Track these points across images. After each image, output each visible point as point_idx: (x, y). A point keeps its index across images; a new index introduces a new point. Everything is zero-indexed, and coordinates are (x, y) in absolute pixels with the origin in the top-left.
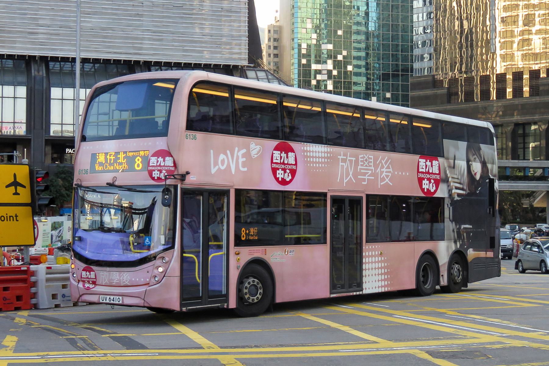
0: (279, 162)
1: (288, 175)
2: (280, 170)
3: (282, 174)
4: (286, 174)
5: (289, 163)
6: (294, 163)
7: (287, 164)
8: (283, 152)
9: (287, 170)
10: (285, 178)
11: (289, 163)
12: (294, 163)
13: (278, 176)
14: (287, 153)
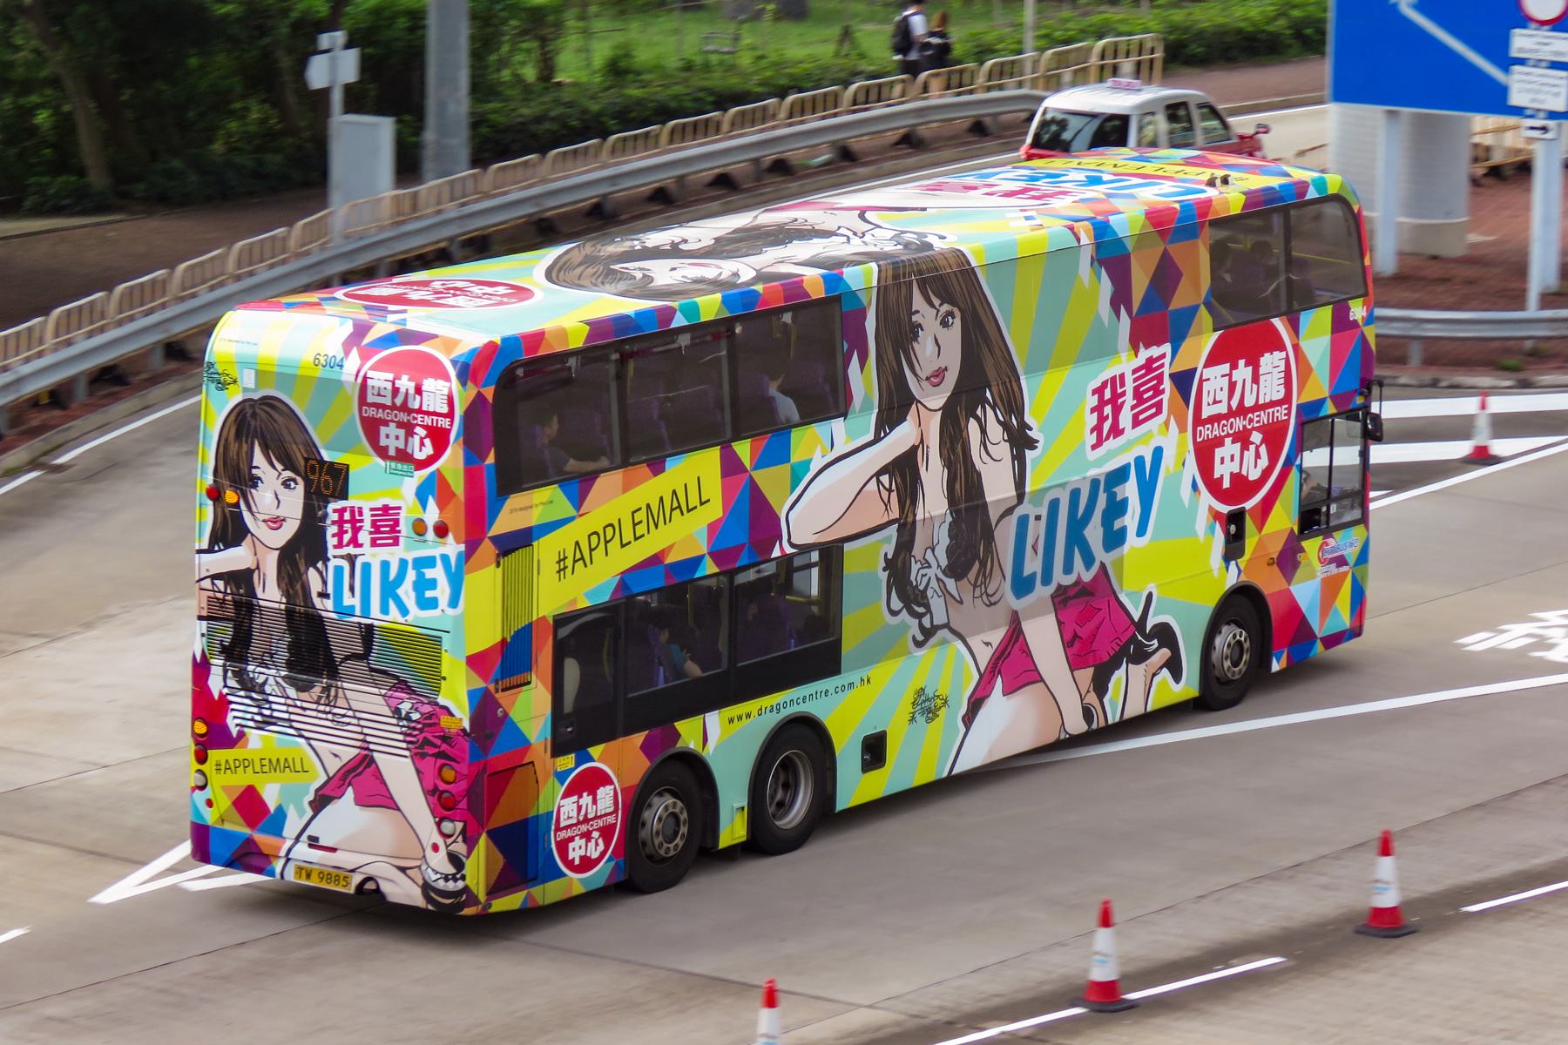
0: (389, 403)
1: (422, 444)
3: (397, 437)
6: (445, 410)
7: (420, 411)
11: (424, 408)
12: (445, 410)
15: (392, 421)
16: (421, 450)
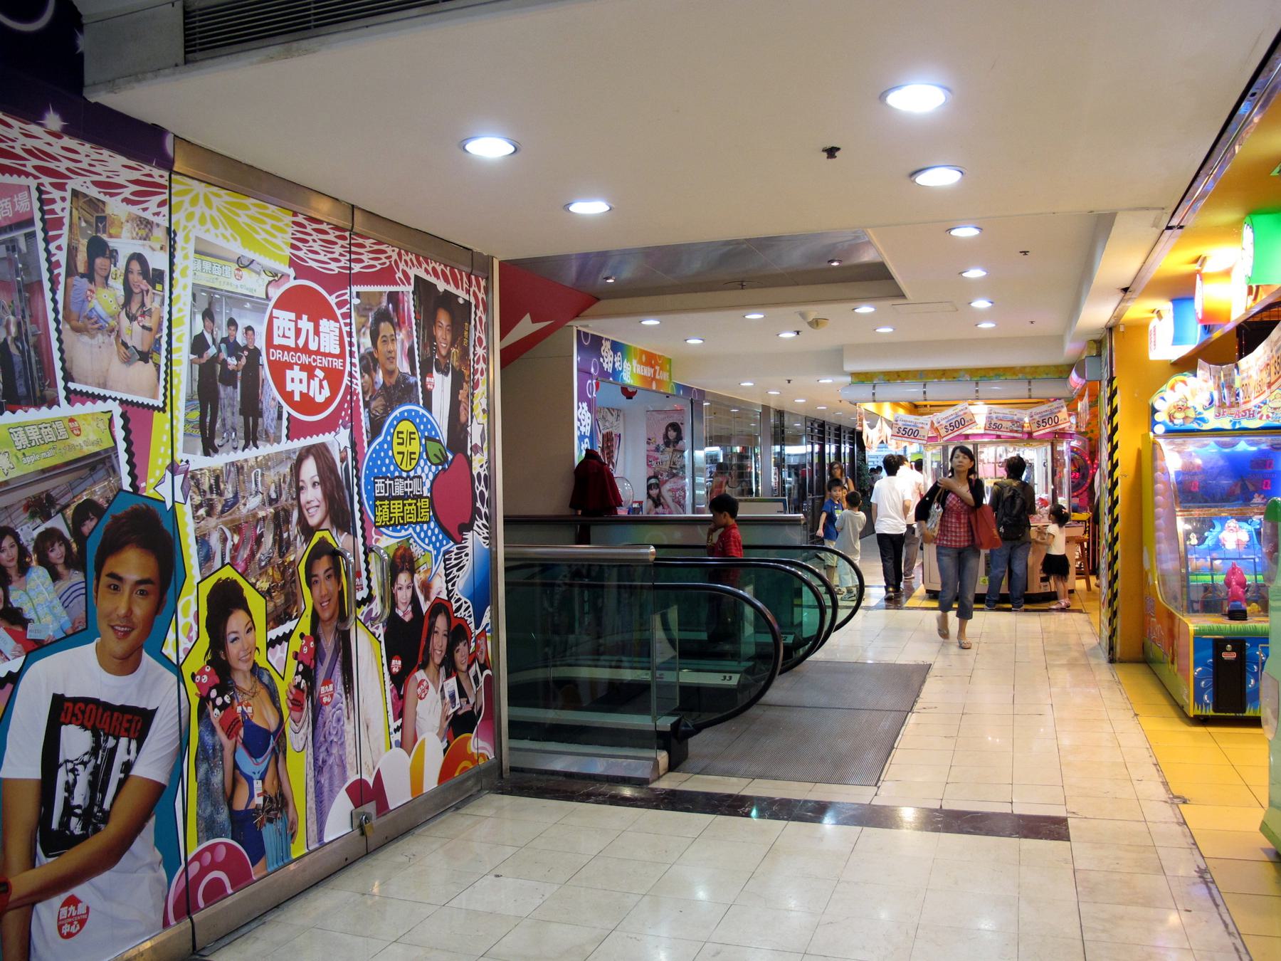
0: (293, 345)
1: (321, 387)
2: (297, 368)
3: (301, 381)
4: (315, 384)
5: (322, 350)
6: (337, 351)
7: (318, 352)
8: (305, 317)
9: (318, 370)
10: (311, 394)
11: (322, 350)
12: (337, 351)
13: (289, 387)
14: (315, 320)
15: (296, 364)
16: (320, 393)
